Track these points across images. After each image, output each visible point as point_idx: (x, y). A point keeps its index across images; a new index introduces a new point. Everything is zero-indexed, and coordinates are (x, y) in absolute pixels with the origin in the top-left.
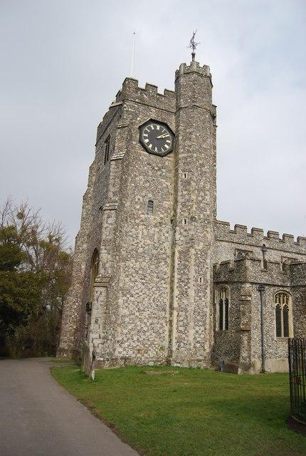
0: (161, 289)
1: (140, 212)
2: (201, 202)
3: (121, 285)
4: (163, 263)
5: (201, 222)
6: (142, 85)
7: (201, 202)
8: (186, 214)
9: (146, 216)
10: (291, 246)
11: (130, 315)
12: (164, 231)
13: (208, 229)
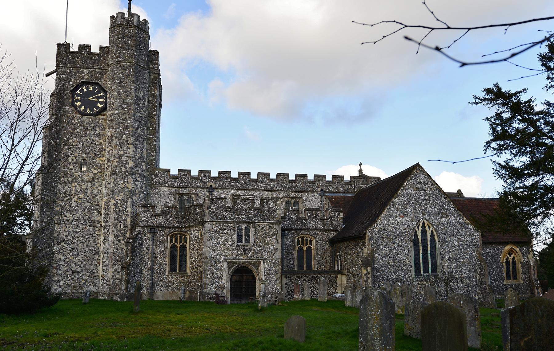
0: (94, 235)
1: (73, 171)
2: (123, 155)
3: (56, 235)
4: (96, 214)
5: (122, 175)
6: (75, 48)
7: (123, 155)
8: (110, 169)
9: (79, 174)
10: (246, 184)
11: (65, 259)
12: (97, 185)
13: (129, 180)
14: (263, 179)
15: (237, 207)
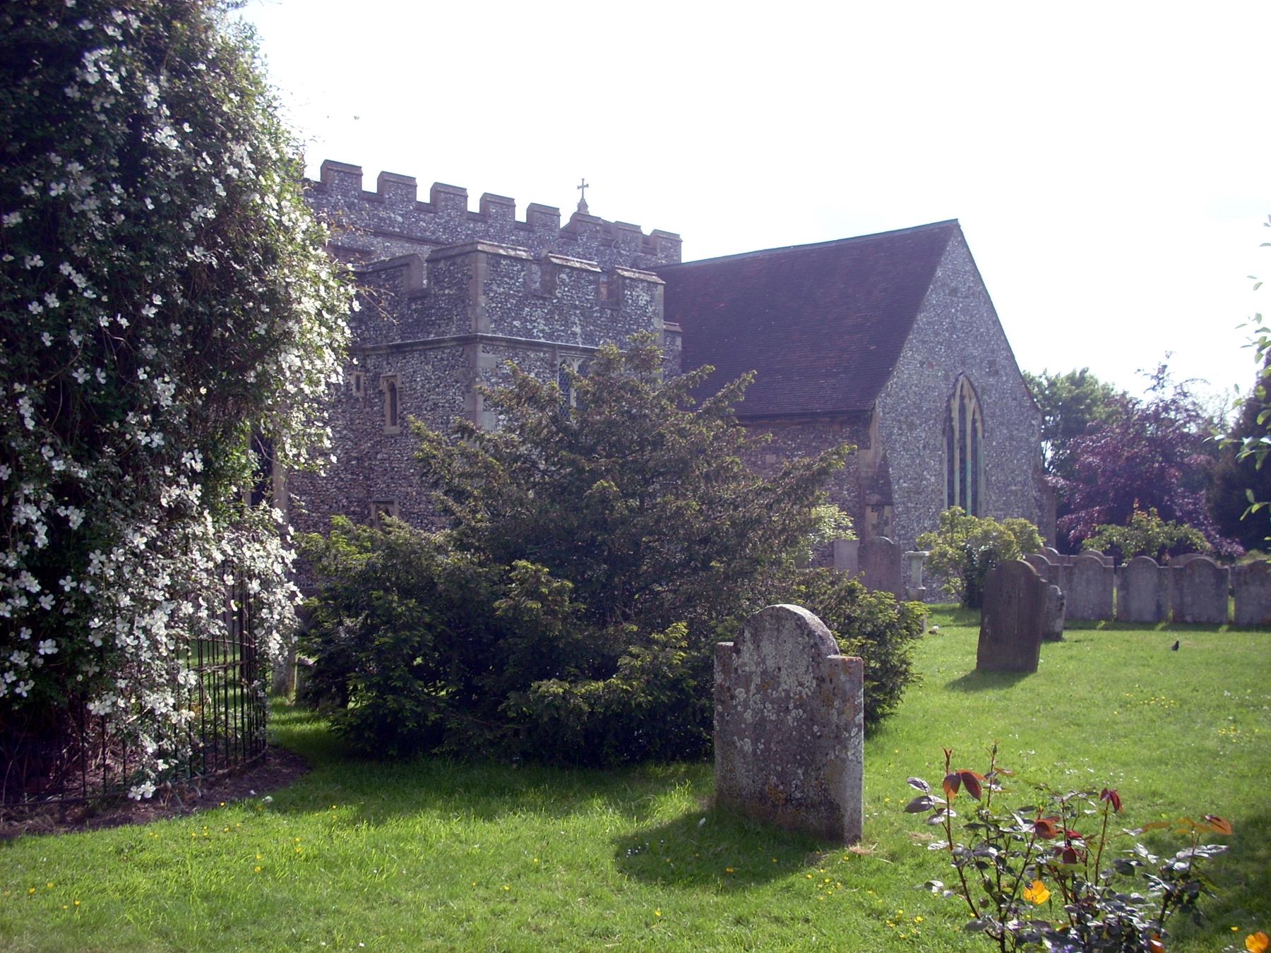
14: (399, 198)
15: (559, 295)
